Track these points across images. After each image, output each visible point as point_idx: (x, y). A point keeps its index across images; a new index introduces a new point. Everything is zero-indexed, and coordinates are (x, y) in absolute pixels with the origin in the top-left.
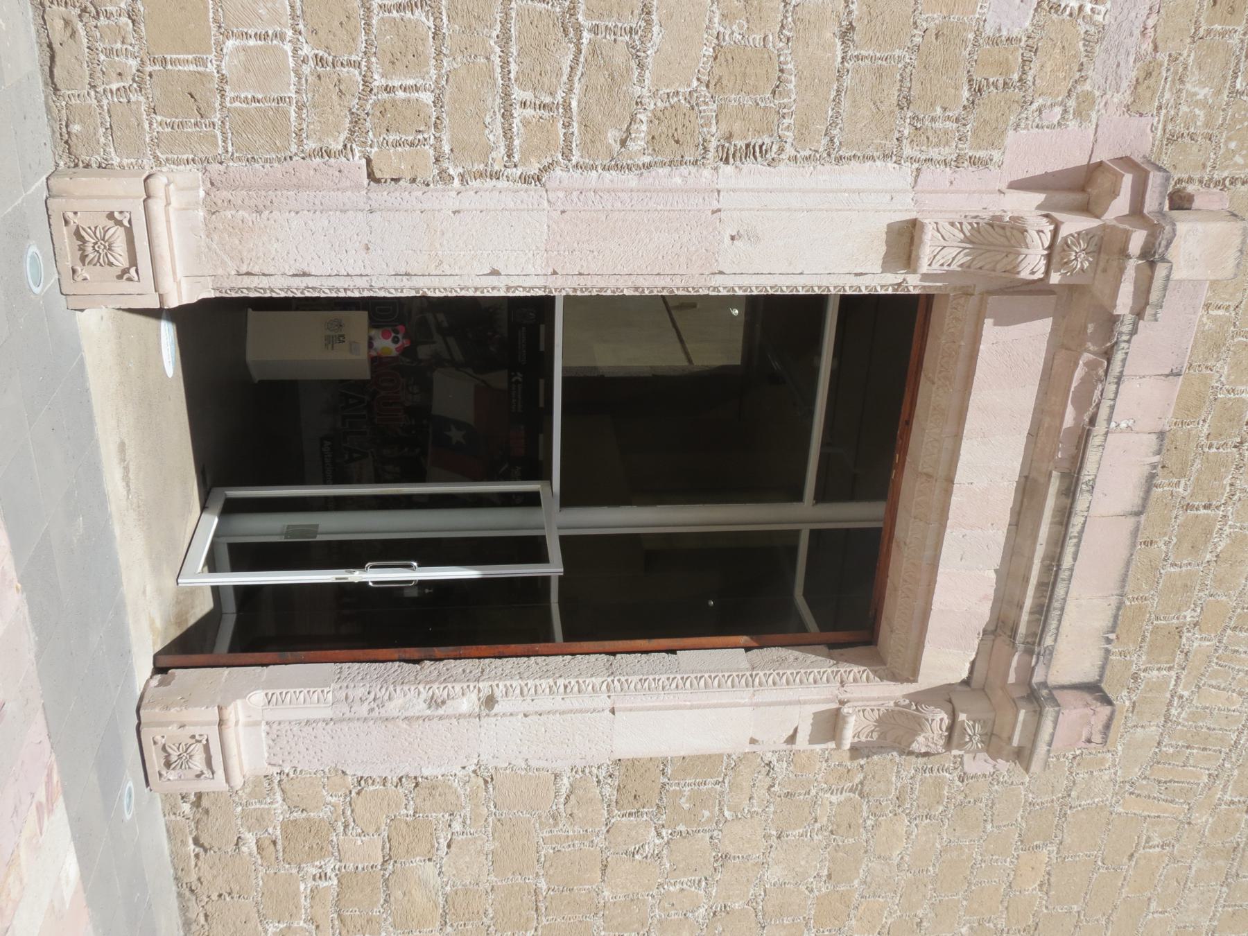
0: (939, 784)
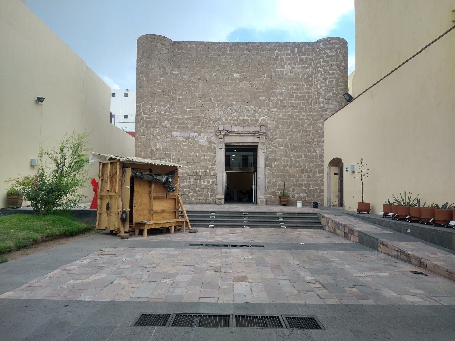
0: (271, 138)
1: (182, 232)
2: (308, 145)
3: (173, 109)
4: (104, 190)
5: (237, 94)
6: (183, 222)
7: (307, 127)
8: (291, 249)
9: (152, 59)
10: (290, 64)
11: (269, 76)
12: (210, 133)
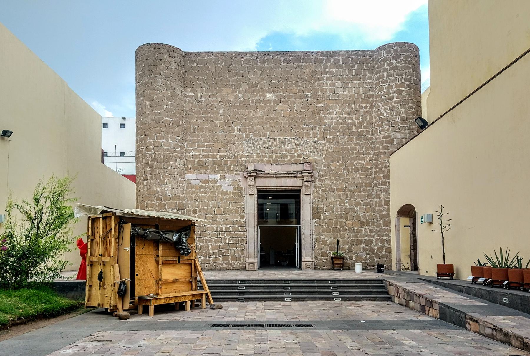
0: (319, 180)
1: (201, 309)
2: (368, 188)
3: (186, 143)
4: (94, 254)
5: (271, 121)
6: (202, 295)
7: (366, 164)
8: (348, 329)
9: (156, 76)
10: (343, 79)
11: (314, 96)
12: (236, 174)
